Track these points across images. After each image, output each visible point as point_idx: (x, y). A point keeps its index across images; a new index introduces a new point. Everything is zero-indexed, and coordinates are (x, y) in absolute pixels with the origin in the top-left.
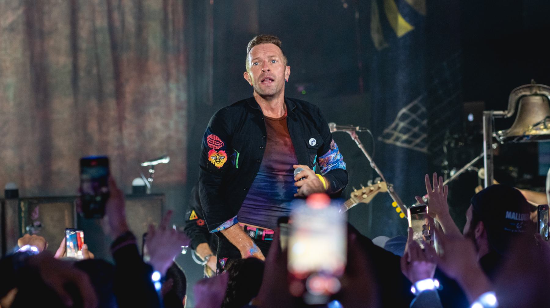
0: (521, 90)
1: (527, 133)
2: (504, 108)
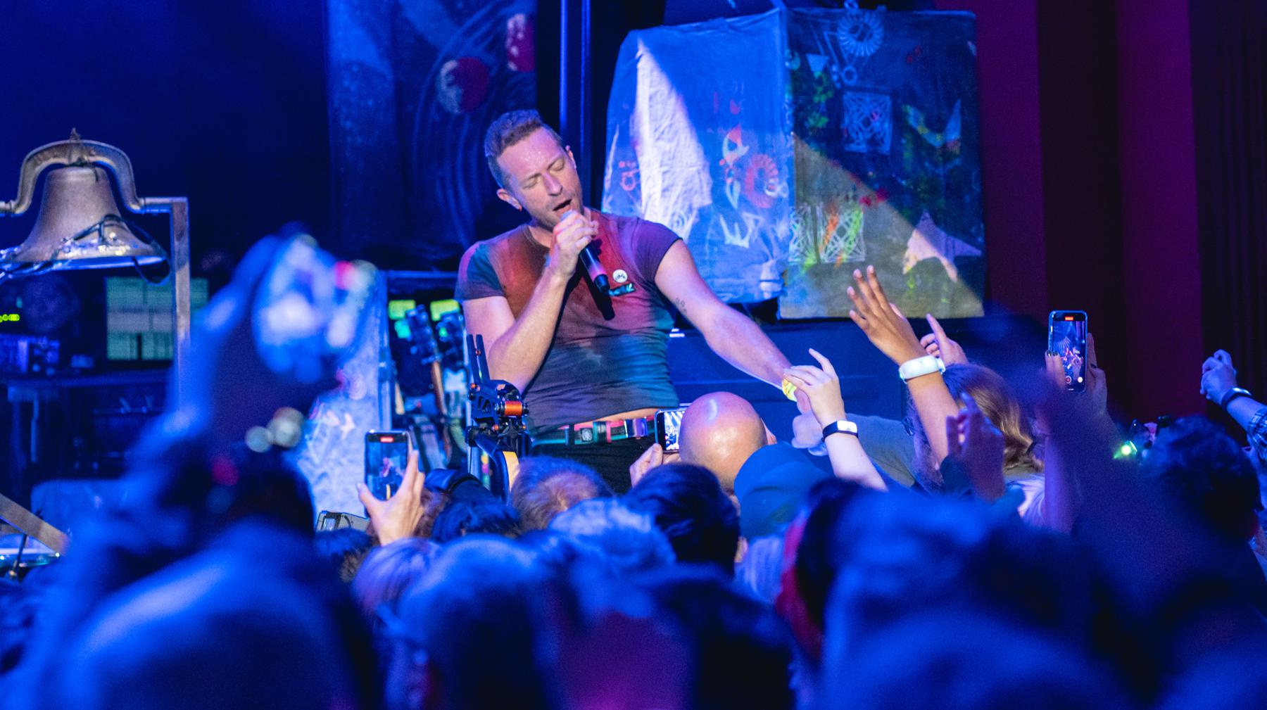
0: (46, 153)
1: (61, 256)
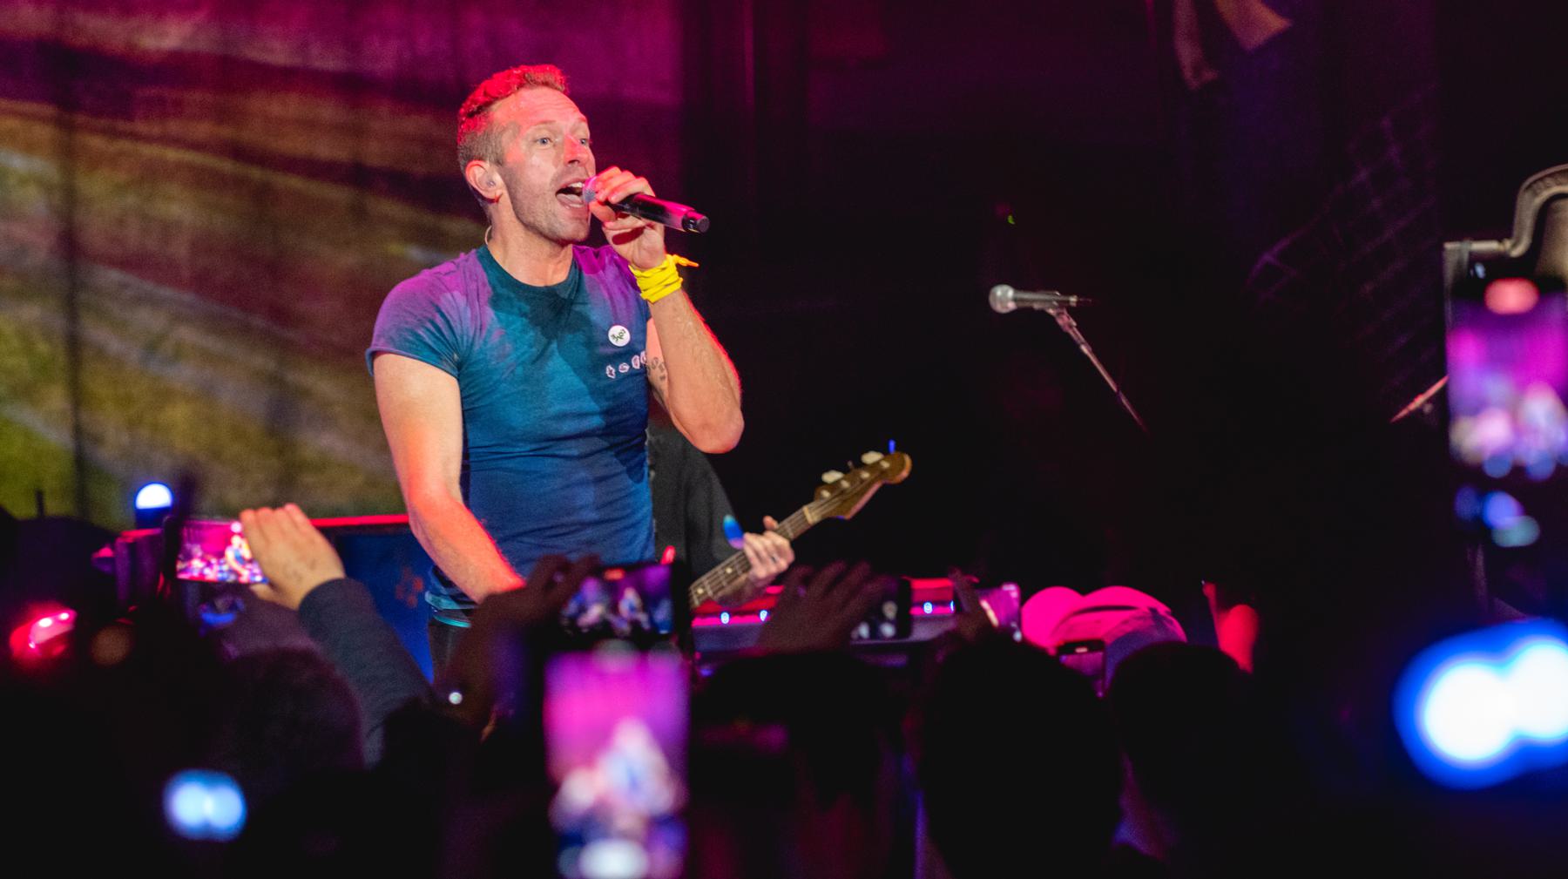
0: (1548, 181)
2: (1503, 230)
